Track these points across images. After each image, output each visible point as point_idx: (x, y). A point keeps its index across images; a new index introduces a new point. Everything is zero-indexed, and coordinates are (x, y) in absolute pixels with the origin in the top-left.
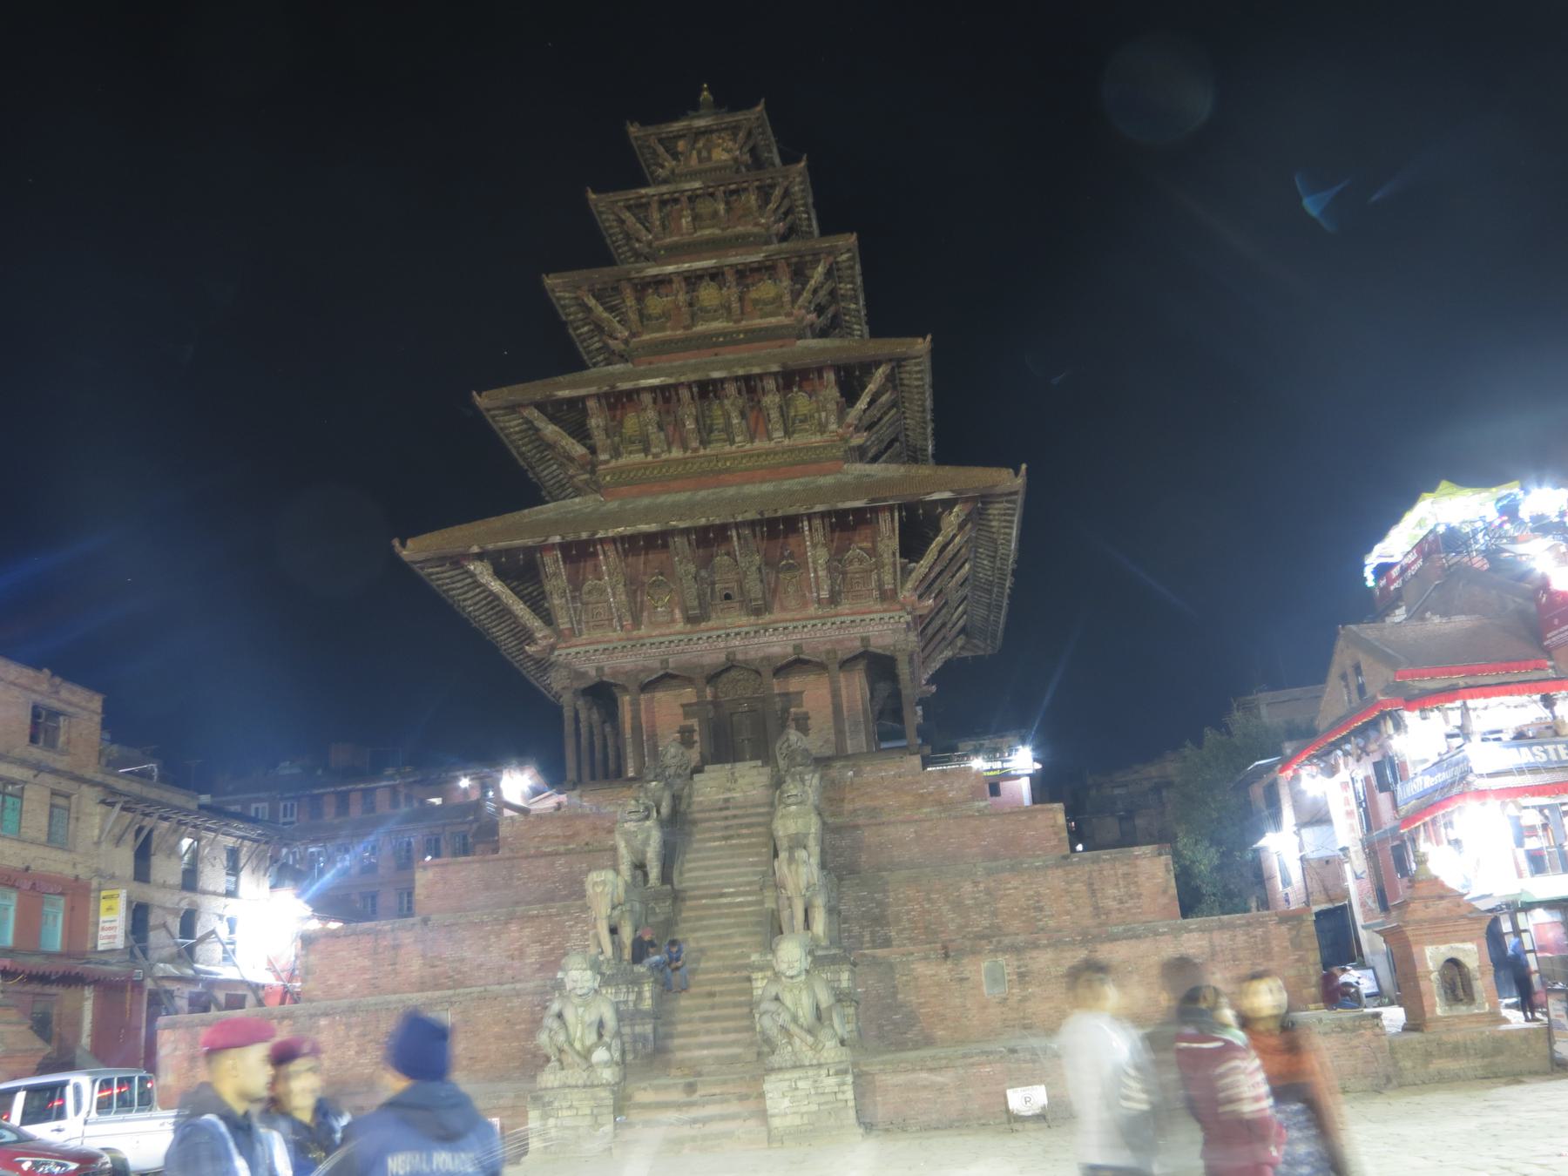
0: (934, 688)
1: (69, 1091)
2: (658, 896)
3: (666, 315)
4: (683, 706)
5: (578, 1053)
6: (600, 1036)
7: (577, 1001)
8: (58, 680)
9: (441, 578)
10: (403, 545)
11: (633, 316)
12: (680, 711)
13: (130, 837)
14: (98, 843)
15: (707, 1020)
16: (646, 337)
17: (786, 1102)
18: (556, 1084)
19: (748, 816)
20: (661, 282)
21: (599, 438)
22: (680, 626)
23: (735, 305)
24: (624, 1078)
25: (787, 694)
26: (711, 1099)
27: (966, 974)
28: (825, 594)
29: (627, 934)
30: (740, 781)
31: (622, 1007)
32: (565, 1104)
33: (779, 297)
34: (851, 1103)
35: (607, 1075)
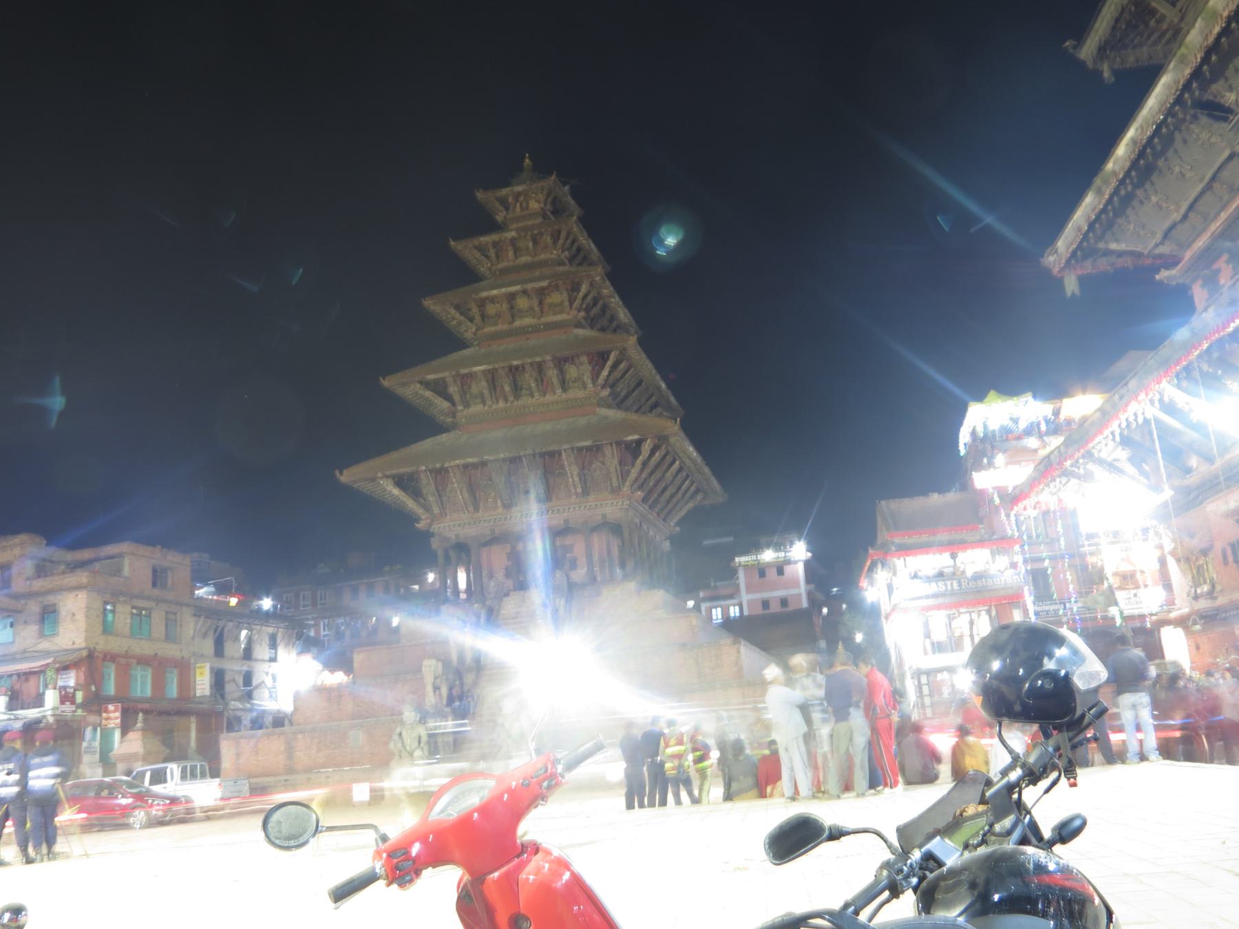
0: (678, 529)
1: (168, 771)
3: (498, 315)
8: (165, 550)
9: (366, 488)
10: (341, 473)
11: (478, 318)
13: (211, 633)
14: (193, 638)
16: (486, 330)
20: (492, 300)
21: (457, 398)
22: (500, 510)
23: (537, 309)
28: (579, 490)
29: (444, 691)
33: (562, 302)
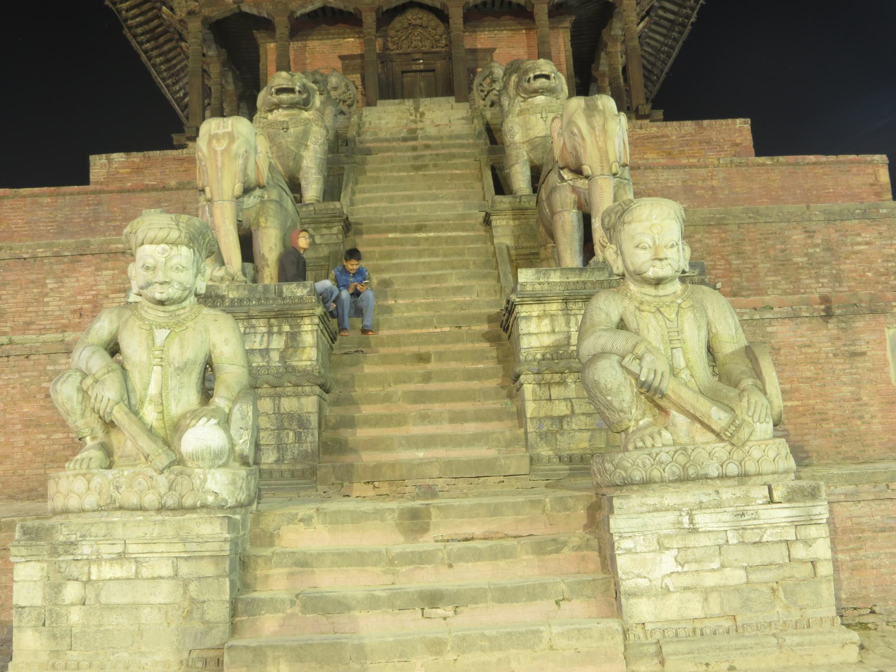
2: (317, 222)
4: (342, 58)
5: (150, 431)
6: (206, 394)
7: (155, 314)
12: (339, 64)
15: (419, 397)
17: (667, 562)
18: (90, 501)
19: (444, 147)
24: (258, 496)
25: (474, 51)
26: (466, 548)
27: (864, 348)
29: (269, 245)
30: (429, 115)
31: (258, 361)
32: (106, 550)
34: (825, 569)
35: (221, 484)
